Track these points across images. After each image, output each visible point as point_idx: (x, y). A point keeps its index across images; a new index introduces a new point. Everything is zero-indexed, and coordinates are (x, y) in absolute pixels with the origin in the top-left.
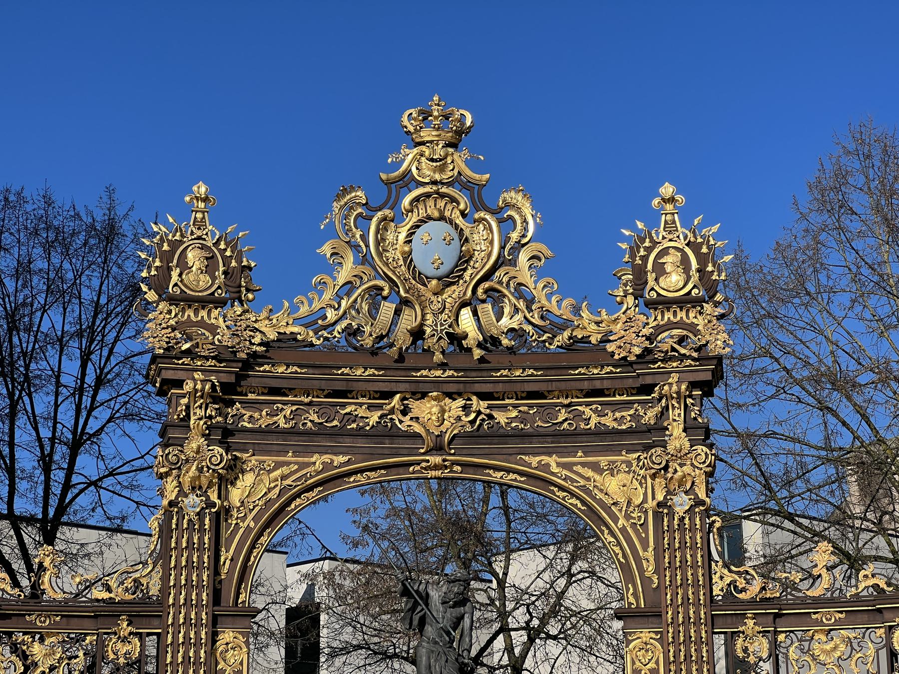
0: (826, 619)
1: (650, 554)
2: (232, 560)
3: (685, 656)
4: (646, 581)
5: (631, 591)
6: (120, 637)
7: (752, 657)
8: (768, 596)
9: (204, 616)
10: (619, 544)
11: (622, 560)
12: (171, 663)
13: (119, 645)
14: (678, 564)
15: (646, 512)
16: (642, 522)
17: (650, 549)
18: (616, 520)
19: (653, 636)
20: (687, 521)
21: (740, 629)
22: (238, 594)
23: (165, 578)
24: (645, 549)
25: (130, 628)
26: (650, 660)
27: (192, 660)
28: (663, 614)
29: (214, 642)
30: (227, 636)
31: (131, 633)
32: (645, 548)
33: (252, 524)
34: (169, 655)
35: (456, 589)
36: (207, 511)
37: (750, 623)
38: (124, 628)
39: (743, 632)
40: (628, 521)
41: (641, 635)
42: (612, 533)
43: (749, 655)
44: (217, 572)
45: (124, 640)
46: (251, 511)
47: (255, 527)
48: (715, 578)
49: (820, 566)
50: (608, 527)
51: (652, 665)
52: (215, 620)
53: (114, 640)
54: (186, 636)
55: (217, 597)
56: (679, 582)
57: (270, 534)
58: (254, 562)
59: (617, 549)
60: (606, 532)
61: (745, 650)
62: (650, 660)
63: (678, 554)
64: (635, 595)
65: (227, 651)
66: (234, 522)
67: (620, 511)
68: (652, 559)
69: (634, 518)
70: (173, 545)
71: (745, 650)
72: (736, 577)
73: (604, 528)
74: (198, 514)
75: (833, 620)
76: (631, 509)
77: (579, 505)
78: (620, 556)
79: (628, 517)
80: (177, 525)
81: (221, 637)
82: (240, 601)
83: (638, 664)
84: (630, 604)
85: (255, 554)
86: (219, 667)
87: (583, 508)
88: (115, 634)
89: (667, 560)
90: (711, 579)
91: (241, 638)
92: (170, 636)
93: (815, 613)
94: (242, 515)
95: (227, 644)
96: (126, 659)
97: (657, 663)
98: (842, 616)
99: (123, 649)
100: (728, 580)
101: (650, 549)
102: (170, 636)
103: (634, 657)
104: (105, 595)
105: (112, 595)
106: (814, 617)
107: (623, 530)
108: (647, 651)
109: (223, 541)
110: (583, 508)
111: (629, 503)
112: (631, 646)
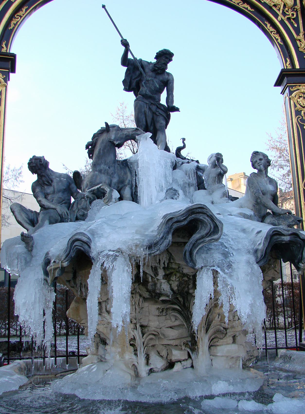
15: (297, 11)
24: (298, 34)
32: (298, 34)
40: (285, 17)
57: (26, 10)
58: (14, 28)
60: (269, 25)
67: (279, 10)
68: (303, 41)
76: (286, 9)
77: (249, 8)
78: (279, 40)
79: (284, 14)
83: (298, 106)
87: (252, 10)
101: (301, 34)
103: (296, 102)
110: (252, 10)
111: (285, 6)
112: (293, 95)
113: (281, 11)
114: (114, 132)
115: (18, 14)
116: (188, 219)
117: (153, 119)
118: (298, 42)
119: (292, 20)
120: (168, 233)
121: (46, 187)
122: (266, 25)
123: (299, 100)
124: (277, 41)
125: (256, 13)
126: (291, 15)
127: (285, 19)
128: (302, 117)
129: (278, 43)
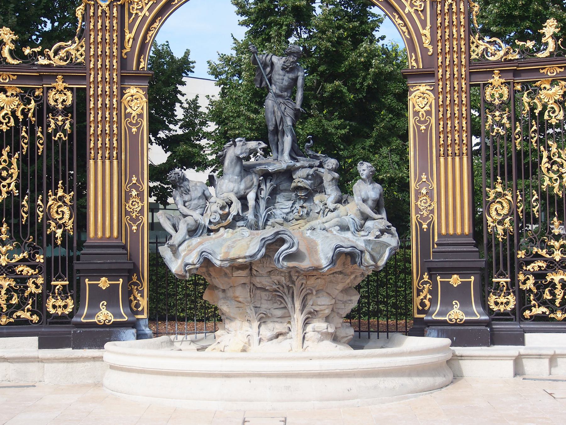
0: (551, 73)
1: (427, 32)
2: (134, 39)
3: (450, 101)
4: (424, 50)
5: (414, 58)
6: (58, 91)
7: (497, 100)
8: (510, 58)
9: (115, 77)
10: (405, 25)
11: (408, 36)
12: (94, 108)
13: (57, 96)
14: (447, 37)
16: (422, 8)
17: (428, 27)
18: (403, 7)
19: (428, 88)
20: (454, 7)
21: (490, 81)
22: (139, 63)
23: (88, 51)
24: (424, 28)
25: (64, 84)
26: (426, 105)
27: (108, 106)
28: (436, 73)
29: (122, 94)
30: (132, 90)
31: (65, 88)
32: (424, 28)
33: (147, 14)
34: (92, 103)
35: (292, 60)
36: (115, 3)
37: (497, 78)
38: (60, 84)
39: (491, 84)
41: (420, 88)
42: (401, 18)
43: (495, 99)
44: (123, 47)
45: (61, 92)
46: (147, 4)
47: (149, 15)
48: (473, 47)
49: (547, 37)
50: (398, 13)
51: (427, 108)
52: (123, 78)
53: (54, 93)
54: (104, 91)
55: (124, 63)
56: (447, 50)
58: (150, 40)
59: (404, 29)
60: (397, 16)
61: (492, 96)
62: (426, 105)
63: (447, 30)
64: (416, 60)
65: (132, 101)
66: (135, 12)
68: (428, 35)
69: (417, 6)
70: (92, 27)
71: (492, 96)
72: (488, 45)
73: (395, 14)
74: (108, 5)
75: (555, 74)
78: (406, 34)
79: (412, 5)
80: (94, 13)
81: (127, 91)
82: (141, 67)
84: (413, 66)
85: (150, 35)
86: (128, 111)
88: (55, 88)
89: (439, 35)
90: (470, 47)
91: (141, 91)
92: (92, 90)
93: (542, 69)
94: (140, 7)
95: (132, 96)
96: (62, 104)
97: (430, 106)
98: (562, 70)
99: (61, 98)
100: (481, 48)
101: (428, 27)
102: (92, 90)
103: (414, 103)
104: (46, 62)
105: (51, 62)
106: (542, 71)
107: (409, 15)
108: (424, 98)
109: (126, 25)
113: (409, 3)
114: (240, 148)
115: (153, 26)
116: (276, 238)
117: (282, 118)
118: (423, 37)
119: (420, 12)
120: (263, 247)
121: (184, 195)
122: (394, 17)
123: (418, 100)
124: (404, 34)
125: (384, 4)
126: (419, 6)
127: (412, 11)
128: (420, 118)
129: (405, 36)
